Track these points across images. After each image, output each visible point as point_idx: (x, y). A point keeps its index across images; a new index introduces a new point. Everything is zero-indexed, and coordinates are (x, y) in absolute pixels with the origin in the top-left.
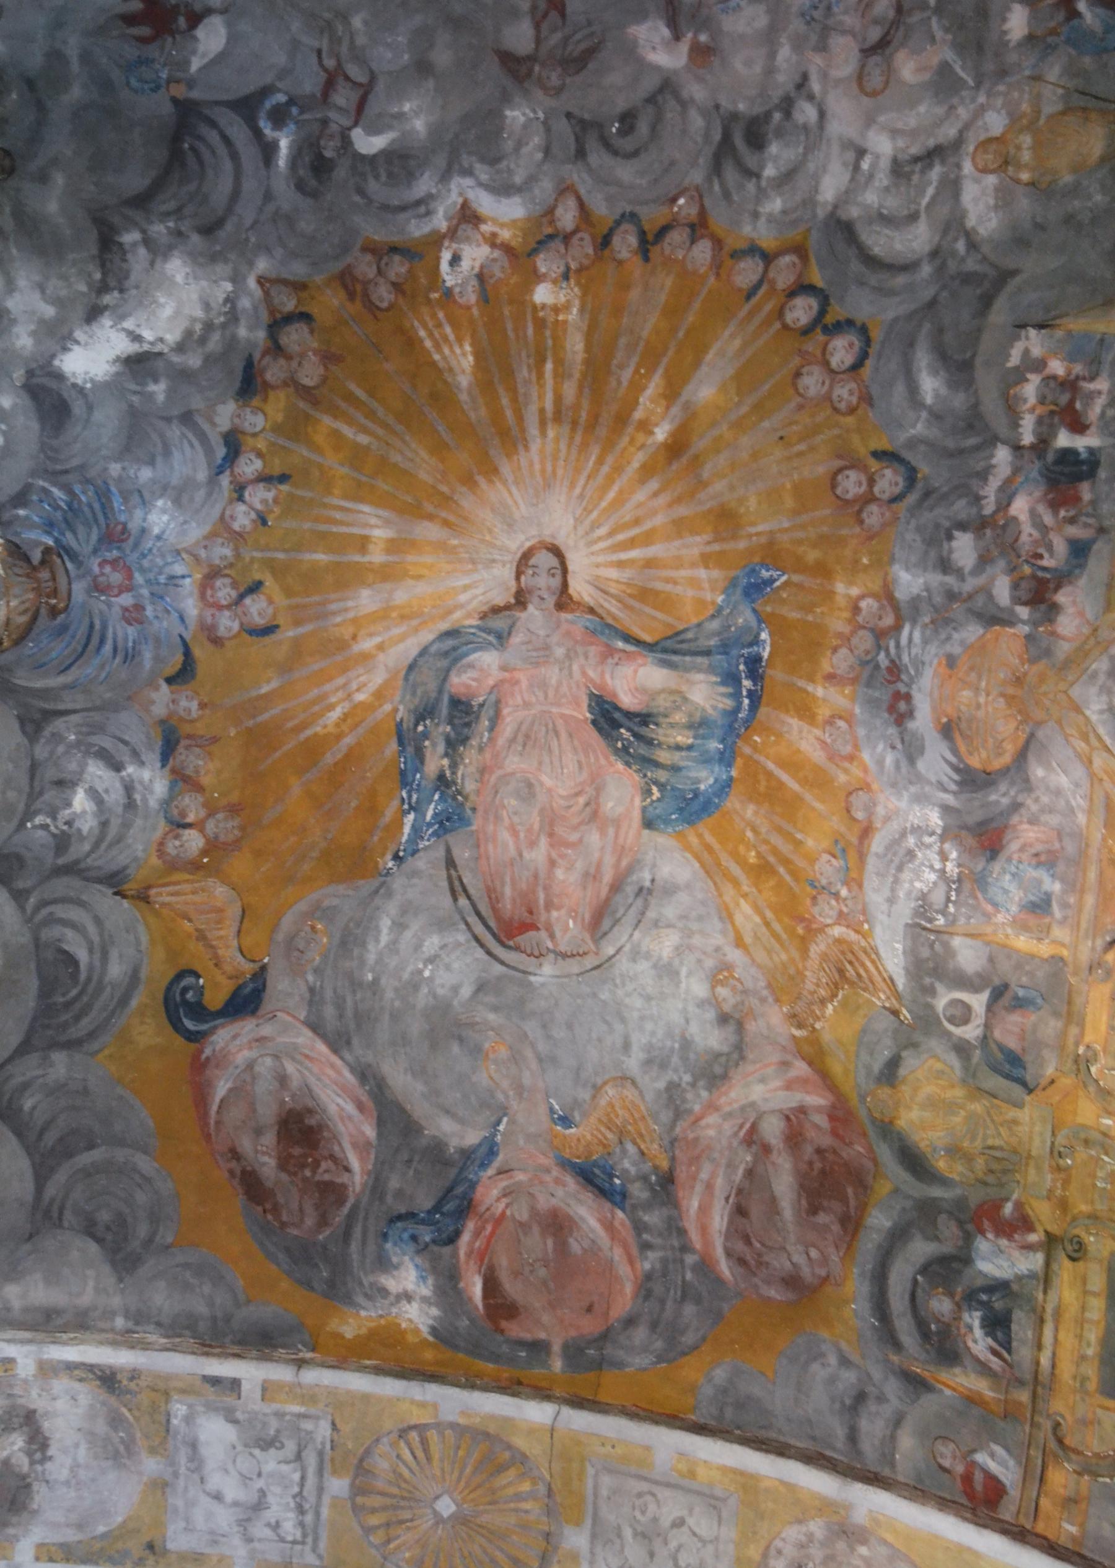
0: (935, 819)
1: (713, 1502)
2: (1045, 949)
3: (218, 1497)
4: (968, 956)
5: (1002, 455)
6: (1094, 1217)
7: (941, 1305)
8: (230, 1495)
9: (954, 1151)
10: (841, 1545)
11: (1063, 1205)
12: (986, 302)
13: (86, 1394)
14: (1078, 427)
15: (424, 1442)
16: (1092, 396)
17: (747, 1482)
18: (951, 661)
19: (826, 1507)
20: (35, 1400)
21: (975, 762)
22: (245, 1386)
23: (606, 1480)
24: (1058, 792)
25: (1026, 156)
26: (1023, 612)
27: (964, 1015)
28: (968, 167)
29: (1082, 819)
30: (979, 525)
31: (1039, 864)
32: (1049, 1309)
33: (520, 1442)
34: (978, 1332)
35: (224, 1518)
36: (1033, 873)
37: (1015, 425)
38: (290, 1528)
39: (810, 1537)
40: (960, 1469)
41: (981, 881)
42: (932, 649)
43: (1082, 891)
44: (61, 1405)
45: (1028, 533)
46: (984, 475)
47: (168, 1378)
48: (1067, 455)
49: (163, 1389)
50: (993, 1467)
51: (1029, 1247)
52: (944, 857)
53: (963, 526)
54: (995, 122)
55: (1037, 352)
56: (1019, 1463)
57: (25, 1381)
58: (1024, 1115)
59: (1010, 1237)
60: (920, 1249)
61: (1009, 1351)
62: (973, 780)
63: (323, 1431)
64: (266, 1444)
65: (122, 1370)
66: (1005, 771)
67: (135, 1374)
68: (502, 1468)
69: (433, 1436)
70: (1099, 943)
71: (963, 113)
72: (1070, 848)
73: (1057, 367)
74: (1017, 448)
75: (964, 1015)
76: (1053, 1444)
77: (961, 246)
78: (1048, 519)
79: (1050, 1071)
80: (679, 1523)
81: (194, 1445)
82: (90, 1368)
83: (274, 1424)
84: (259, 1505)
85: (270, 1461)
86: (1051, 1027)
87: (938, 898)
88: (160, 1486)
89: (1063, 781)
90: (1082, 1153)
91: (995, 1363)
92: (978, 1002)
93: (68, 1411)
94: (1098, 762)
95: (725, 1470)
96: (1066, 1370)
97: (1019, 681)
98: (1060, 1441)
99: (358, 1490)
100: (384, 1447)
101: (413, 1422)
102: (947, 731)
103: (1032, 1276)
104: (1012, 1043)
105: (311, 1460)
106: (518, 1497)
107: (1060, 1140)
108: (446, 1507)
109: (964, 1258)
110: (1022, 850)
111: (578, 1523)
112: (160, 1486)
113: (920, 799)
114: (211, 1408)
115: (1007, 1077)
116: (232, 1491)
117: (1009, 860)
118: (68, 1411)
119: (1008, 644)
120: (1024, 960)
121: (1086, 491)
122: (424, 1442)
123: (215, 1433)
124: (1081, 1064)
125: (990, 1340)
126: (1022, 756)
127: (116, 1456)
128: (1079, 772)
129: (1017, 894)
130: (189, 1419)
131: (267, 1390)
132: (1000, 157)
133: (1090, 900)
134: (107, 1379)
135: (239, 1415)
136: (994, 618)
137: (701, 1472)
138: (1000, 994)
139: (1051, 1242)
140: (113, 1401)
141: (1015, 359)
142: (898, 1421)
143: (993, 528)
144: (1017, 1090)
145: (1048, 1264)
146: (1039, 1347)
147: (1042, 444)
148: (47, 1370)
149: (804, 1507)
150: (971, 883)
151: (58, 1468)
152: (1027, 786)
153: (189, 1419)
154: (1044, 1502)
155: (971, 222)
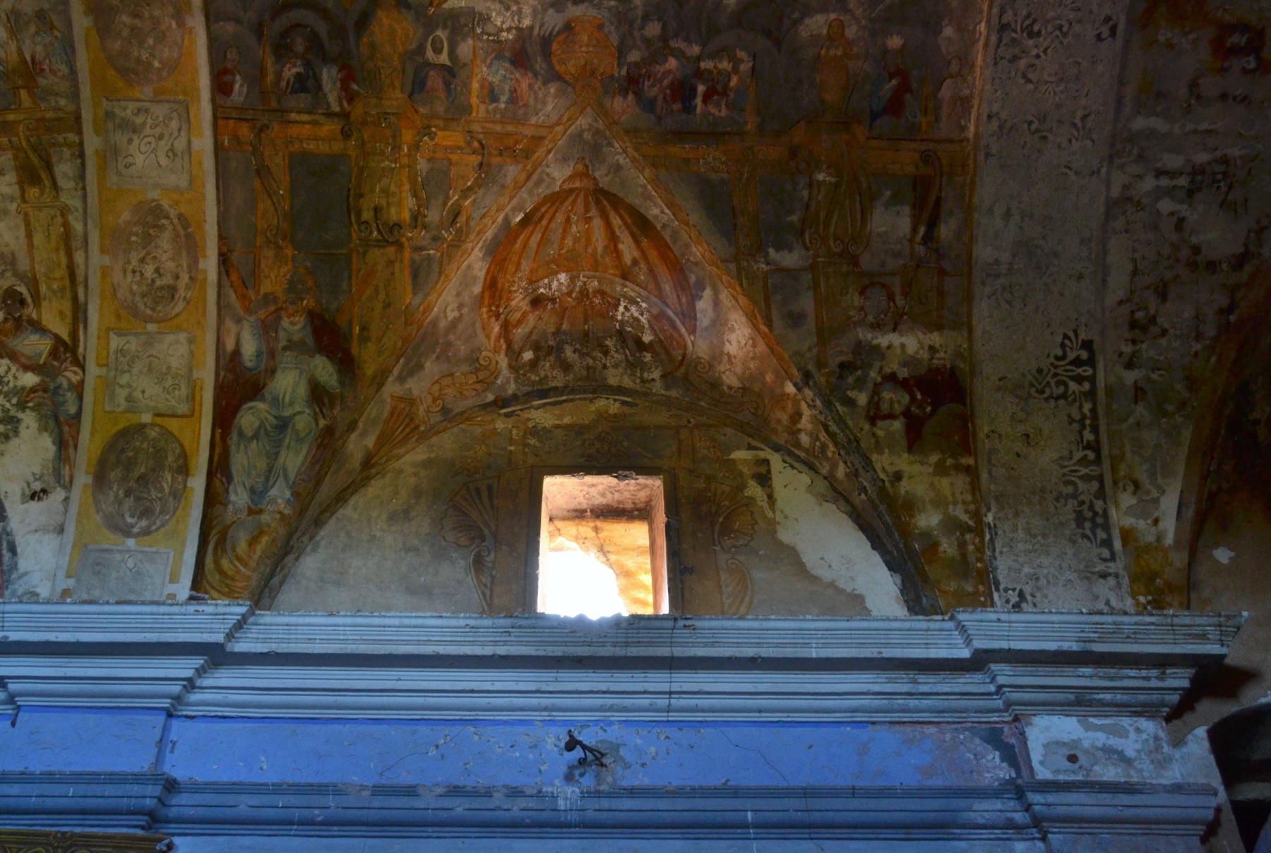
0: (526, 22)
2: (474, 100)
4: (465, 48)
5: (696, 50)
6: (363, 143)
7: (300, 47)
9: (372, 46)
11: (364, 123)
12: (768, 34)
14: (707, 98)
16: (718, 105)
18: (600, 27)
21: (555, 46)
24: (544, 103)
25: (832, 52)
26: (624, 72)
27: (438, 51)
28: (833, 16)
29: (533, 120)
30: (664, 38)
31: (511, 92)
32: (316, 117)
34: (294, 70)
36: (507, 87)
37: (712, 56)
40: (229, 65)
41: (499, 56)
42: (606, 14)
43: (501, 122)
45: (659, 69)
46: (688, 40)
48: (694, 90)
50: (237, 86)
51: (341, 105)
52: (509, 30)
53: (664, 28)
54: (851, 32)
55: (742, 67)
58: (398, 94)
59: (342, 88)
60: (322, 28)
61: (291, 93)
62: (546, 43)
66: (551, 66)
70: (481, 136)
71: (859, 12)
72: (521, 112)
73: (734, 81)
74: (699, 59)
75: (438, 51)
77: (796, 15)
78: (666, 82)
79: (421, 110)
86: (440, 109)
87: (490, 28)
89: (550, 107)
90: (388, 133)
91: (283, 84)
92: (444, 58)
94: (559, 129)
96: (294, 131)
97: (593, 73)
98: (261, 130)
102: (568, 27)
103: (328, 105)
104: (429, 83)
107: (393, 119)
109: (326, 59)
110: (518, 81)
113: (535, 12)
115: (414, 83)
117: (512, 73)
119: (607, 64)
120: (467, 85)
121: (677, 106)
124: (426, 130)
125: (292, 80)
126: (558, 77)
128: (554, 118)
129: (495, 79)
132: (836, 35)
133: (498, 128)
136: (621, 52)
138: (449, 72)
139: (345, 115)
141: (741, 54)
142: (238, 21)
143: (659, 50)
144: (408, 88)
145: (336, 115)
146: (299, 112)
147: (699, 74)
150: (498, 50)
152: (545, 83)
154: (231, 122)
155: (807, 21)
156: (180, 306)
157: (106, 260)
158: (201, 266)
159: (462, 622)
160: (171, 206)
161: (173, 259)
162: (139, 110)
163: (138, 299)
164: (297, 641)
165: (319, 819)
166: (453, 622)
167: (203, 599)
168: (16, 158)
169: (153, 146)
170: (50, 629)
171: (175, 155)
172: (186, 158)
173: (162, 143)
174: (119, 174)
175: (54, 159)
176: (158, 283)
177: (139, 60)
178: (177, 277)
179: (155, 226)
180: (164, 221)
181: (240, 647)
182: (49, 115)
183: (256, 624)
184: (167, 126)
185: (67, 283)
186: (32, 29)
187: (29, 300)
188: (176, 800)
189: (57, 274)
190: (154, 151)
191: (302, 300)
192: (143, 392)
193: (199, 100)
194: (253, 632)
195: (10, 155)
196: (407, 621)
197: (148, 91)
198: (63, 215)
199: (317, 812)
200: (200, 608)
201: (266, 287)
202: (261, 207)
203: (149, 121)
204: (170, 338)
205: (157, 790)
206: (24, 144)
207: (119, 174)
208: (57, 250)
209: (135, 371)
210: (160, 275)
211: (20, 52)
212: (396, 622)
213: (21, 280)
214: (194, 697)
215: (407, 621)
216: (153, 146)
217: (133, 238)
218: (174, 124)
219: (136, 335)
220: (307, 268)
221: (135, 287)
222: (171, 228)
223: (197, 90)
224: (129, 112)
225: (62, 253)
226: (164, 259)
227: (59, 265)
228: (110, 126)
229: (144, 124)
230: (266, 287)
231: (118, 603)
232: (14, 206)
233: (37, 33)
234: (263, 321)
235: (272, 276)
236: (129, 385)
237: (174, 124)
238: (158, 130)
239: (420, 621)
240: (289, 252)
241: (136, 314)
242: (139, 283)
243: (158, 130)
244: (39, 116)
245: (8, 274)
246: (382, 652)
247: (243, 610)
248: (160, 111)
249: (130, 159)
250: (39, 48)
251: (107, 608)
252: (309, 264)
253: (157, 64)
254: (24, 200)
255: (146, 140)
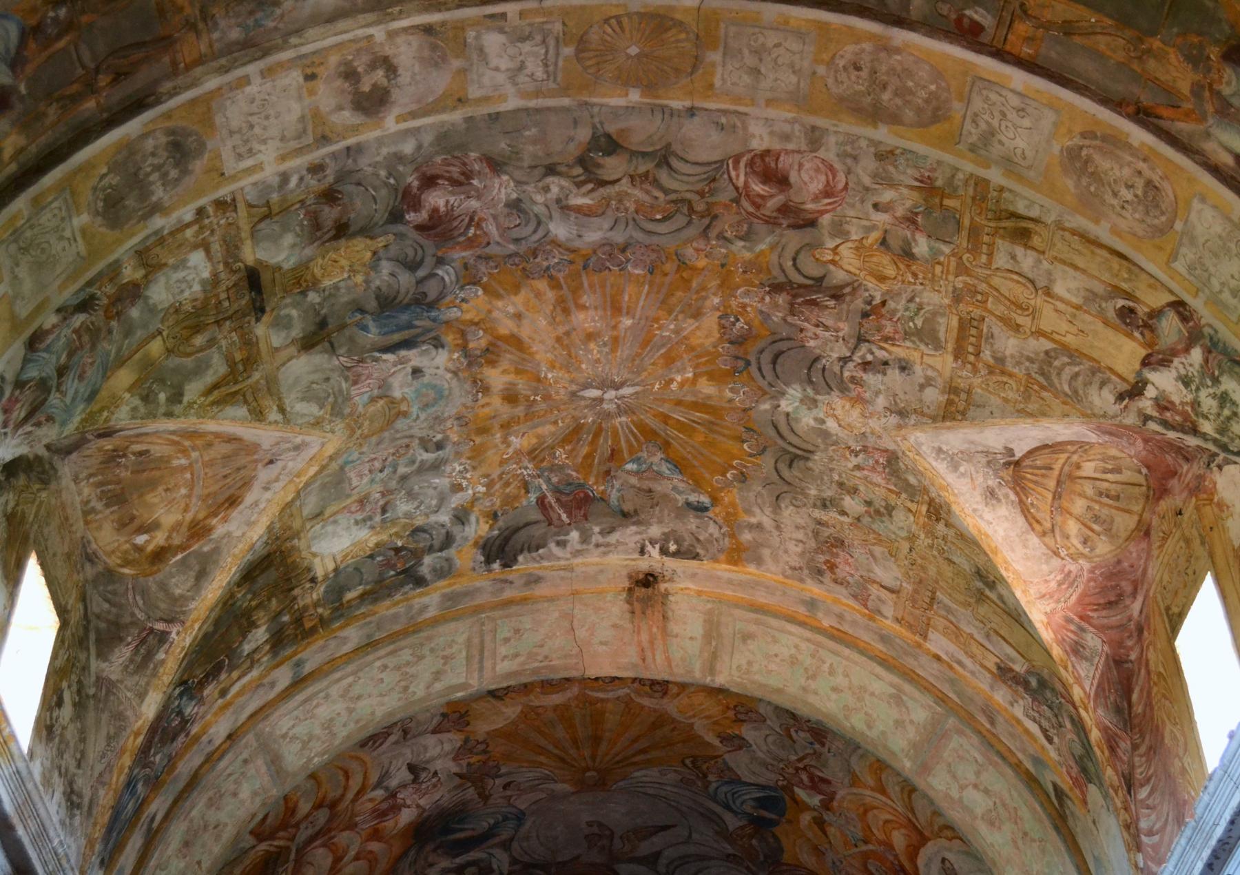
1: (800, 35)
3: (497, 69)
8: (503, 67)
10: (883, 55)
13: (415, 40)
15: (619, 23)
17: (823, 27)
19: (872, 37)
20: (388, 51)
22: (509, 15)
23: (733, 29)
33: (678, 16)
35: (501, 78)
38: (540, 74)
39: (863, 51)
40: (953, 16)
44: (403, 49)
47: (463, 21)
49: (460, 27)
50: (976, 17)
56: (994, 17)
57: (381, 44)
63: (558, 27)
64: (523, 39)
65: (436, 23)
67: (443, 24)
68: (667, 30)
69: (625, 20)
76: (1018, 12)
80: (778, 45)
81: (481, 50)
82: (417, 27)
83: (528, 29)
84: (522, 67)
85: (526, 47)
88: (463, 72)
93: (406, 53)
95: (808, 21)
98: (1025, 12)
99: (579, 51)
100: (595, 28)
101: (613, 14)
105: (551, 42)
106: (678, 41)
108: (633, 51)
111: (715, 48)
112: (463, 72)
114: (488, 29)
116: (504, 64)
118: (406, 53)
122: (619, 23)
123: (493, 41)
127: (436, 65)
130: (477, 38)
131: (522, 14)
134: (428, 30)
135: (507, 29)
137: (792, 21)
140: (432, 39)
148: (392, 35)
149: (857, 36)
151: (404, 77)
153: (477, 38)
154: (1009, 36)
156: (1166, 185)
157: (1105, 225)
158: (1136, 144)
160: (1071, 139)
161: (1121, 167)
162: (974, 121)
163: (1149, 220)
168: (1003, 237)
169: (1010, 125)
171: (1023, 110)
172: (1028, 101)
173: (1009, 116)
174: (1029, 168)
175: (1011, 208)
176: (1139, 192)
177: (927, 101)
178: (1140, 173)
179: (1086, 162)
180: (1084, 152)
182: (971, 191)
184: (994, 104)
185: (1124, 262)
186: (891, 168)
187: (1131, 304)
189: (1116, 266)
190: (1016, 127)
191: (1208, 58)
192: (1233, 277)
193: (976, 65)
195: (999, 241)
197: (957, 105)
198: (1064, 229)
201: (1184, 87)
202: (1102, 47)
203: (986, 117)
204: (1193, 216)
206: (992, 224)
207: (1029, 168)
208: (1093, 252)
209: (1212, 269)
210: (1132, 186)
211: (912, 188)
213: (1113, 298)
216: (1010, 125)
217: (1092, 189)
218: (993, 96)
219: (1181, 244)
220: (1178, 35)
221: (1137, 216)
222: (1091, 151)
223: (964, 62)
224: (973, 131)
225: (1099, 251)
226: (1118, 174)
227: (1107, 260)
228: (983, 152)
229: (987, 123)
230: (1184, 87)
232: (1045, 262)
233: (896, 167)
234: (1217, 112)
235: (1175, 74)
236: (1223, 284)
237: (993, 96)
238: (996, 114)
240: (1156, 44)
241: (1161, 231)
242: (1135, 210)
243: (996, 114)
244: (969, 201)
245: (1104, 305)
248: (977, 104)
249: (1019, 152)
250: (909, 171)
252: (1175, 30)
253: (933, 87)
254: (1044, 253)
255: (1003, 128)
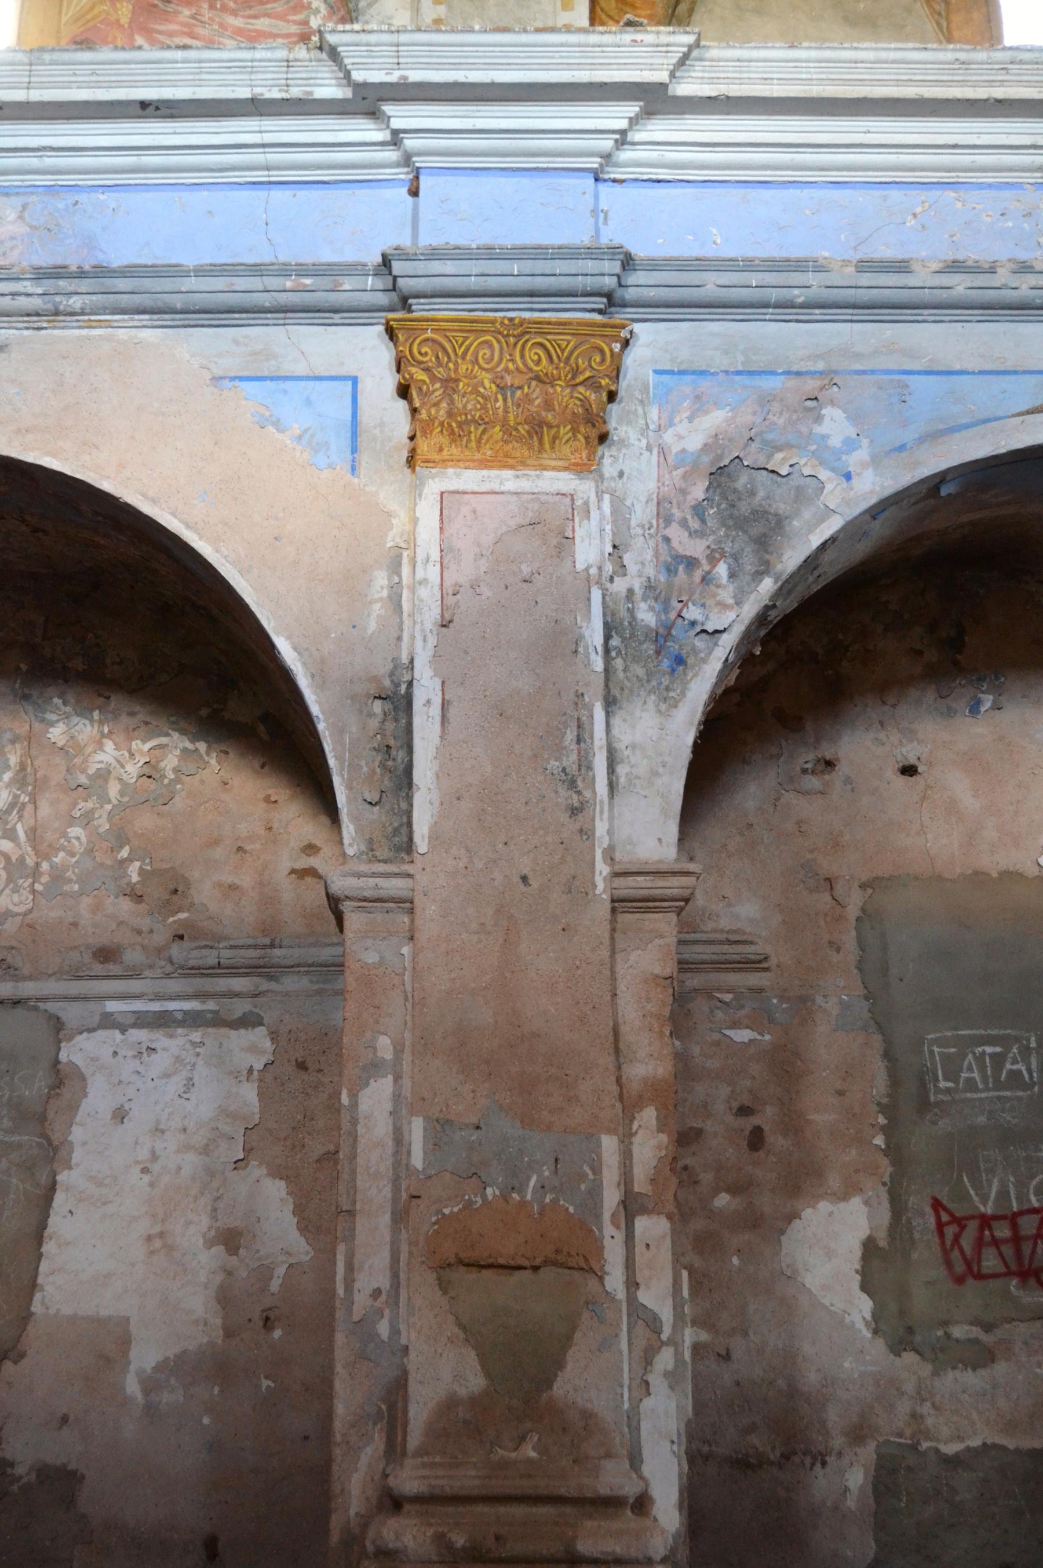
159: (950, 56)
164: (751, 81)
165: (800, 300)
166: (941, 56)
167: (641, 25)
170: (456, 66)
181: (683, 89)
183: (701, 60)
188: (632, 279)
194: (697, 70)
196: (883, 55)
199: (796, 291)
200: (639, 37)
205: (616, 267)
212: (871, 55)
214: (626, 155)
215: (883, 55)
231: (538, 30)
239: (899, 55)
246: (855, 95)
247: (690, 39)
251: (524, 38)
